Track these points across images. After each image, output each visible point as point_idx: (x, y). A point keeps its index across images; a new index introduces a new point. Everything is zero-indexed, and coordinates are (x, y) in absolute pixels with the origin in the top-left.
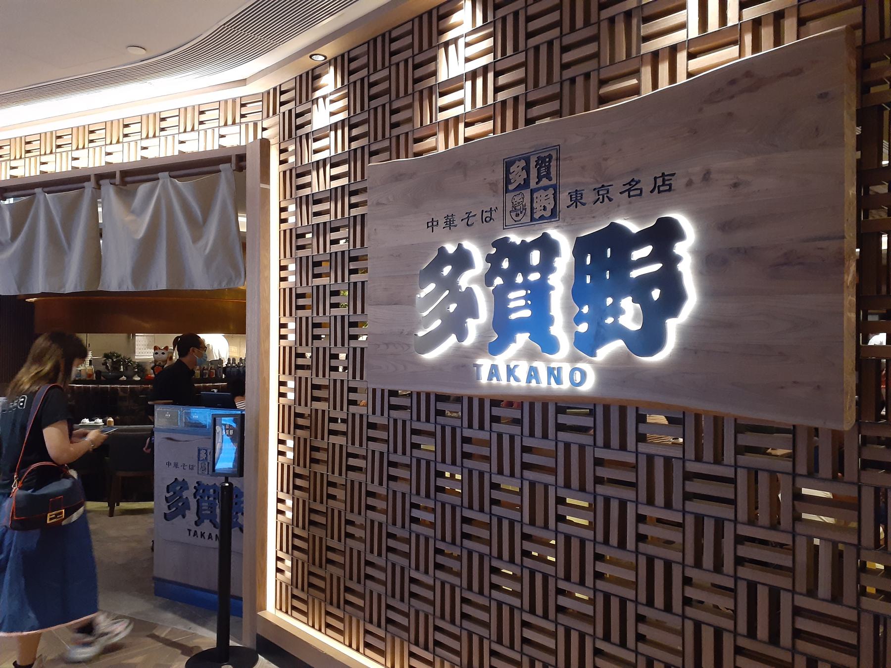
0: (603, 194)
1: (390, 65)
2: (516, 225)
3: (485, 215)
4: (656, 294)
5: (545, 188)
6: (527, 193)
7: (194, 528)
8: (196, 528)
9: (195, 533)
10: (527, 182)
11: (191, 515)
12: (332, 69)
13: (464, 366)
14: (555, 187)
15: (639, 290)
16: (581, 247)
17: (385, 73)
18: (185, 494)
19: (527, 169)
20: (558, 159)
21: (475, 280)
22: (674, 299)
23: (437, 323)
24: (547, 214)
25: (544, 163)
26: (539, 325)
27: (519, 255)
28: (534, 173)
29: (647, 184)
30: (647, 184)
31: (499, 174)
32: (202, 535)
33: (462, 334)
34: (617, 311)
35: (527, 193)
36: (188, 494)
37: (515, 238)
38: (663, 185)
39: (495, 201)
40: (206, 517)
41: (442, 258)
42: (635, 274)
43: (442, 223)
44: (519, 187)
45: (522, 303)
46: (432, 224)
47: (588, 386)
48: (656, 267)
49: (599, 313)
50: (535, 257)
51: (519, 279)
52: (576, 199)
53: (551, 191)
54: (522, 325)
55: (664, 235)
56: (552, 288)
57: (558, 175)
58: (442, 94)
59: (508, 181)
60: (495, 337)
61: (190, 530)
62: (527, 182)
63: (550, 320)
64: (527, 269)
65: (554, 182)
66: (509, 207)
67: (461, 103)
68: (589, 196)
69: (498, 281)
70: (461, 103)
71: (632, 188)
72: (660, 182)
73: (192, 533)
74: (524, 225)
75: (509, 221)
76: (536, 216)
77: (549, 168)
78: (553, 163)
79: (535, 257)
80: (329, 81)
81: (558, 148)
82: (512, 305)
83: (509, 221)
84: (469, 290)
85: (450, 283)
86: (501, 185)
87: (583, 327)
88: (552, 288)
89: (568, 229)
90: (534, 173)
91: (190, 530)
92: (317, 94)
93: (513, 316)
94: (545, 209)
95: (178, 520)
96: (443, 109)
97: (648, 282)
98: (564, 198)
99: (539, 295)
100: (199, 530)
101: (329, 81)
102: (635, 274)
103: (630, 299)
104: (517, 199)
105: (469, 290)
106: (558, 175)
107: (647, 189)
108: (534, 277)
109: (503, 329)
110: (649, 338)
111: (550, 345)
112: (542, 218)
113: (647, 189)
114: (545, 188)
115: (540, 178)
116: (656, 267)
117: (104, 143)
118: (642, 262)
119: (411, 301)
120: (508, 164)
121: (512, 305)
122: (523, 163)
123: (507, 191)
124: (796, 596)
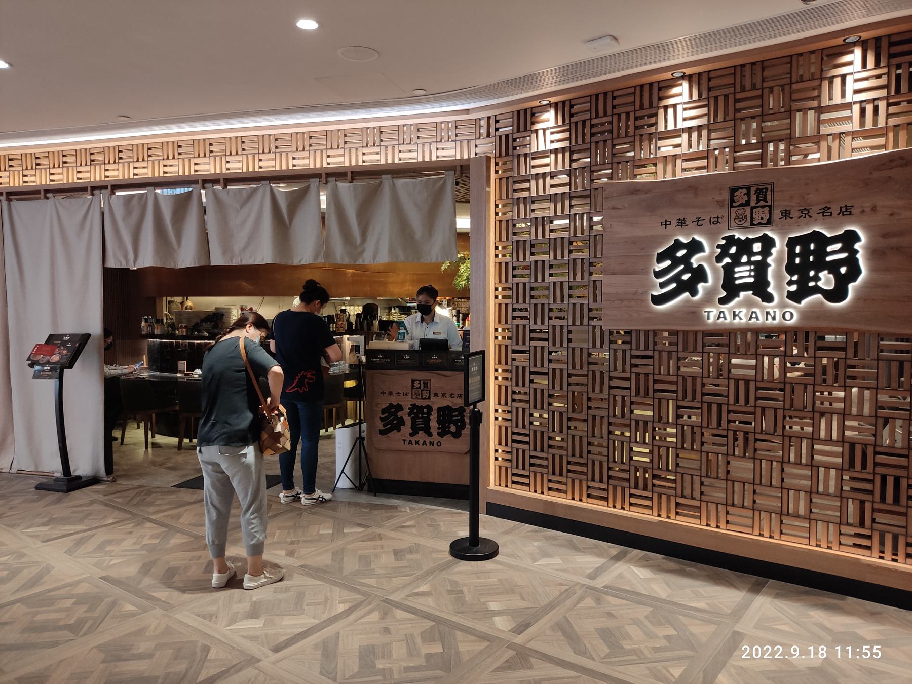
0: (805, 213)
1: (612, 115)
2: (739, 227)
3: (712, 220)
4: (843, 270)
5: (763, 207)
6: (748, 209)
7: (409, 438)
8: (411, 438)
9: (410, 442)
10: (748, 203)
11: (406, 429)
12: (552, 112)
13: (693, 312)
14: (770, 207)
15: (833, 267)
16: (792, 243)
17: (609, 119)
18: (400, 414)
19: (748, 194)
20: (772, 191)
21: (708, 259)
22: (854, 272)
23: (674, 285)
24: (764, 221)
25: (762, 193)
26: (760, 288)
27: (745, 247)
28: (753, 197)
29: (835, 210)
30: (835, 210)
31: (726, 195)
32: (417, 443)
33: (694, 293)
34: (816, 278)
35: (748, 209)
36: (404, 414)
37: (739, 235)
38: (846, 212)
39: (723, 212)
40: (421, 429)
41: (678, 245)
42: (829, 259)
43: (675, 223)
44: (741, 205)
45: (747, 274)
46: (666, 224)
47: (793, 322)
48: (843, 255)
49: (803, 283)
50: (757, 247)
51: (744, 259)
52: (786, 214)
53: (767, 209)
54: (745, 287)
55: (849, 239)
56: (769, 265)
57: (772, 200)
58: (534, 159)
59: (732, 201)
60: (724, 294)
61: (404, 441)
62: (748, 203)
63: (767, 284)
64: (751, 254)
65: (769, 203)
66: (733, 215)
67: (548, 165)
68: (795, 213)
69: (727, 260)
70: (548, 165)
71: (825, 212)
72: (843, 210)
73: (407, 443)
74: (746, 227)
75: (733, 224)
76: (755, 223)
77: (765, 195)
78: (769, 193)
79: (757, 247)
80: (549, 119)
81: (772, 184)
82: (736, 275)
83: (733, 224)
84: (700, 267)
85: (686, 260)
86: (727, 202)
87: (794, 288)
88: (769, 265)
89: (782, 234)
90: (753, 197)
91: (404, 441)
92: (538, 126)
93: (737, 282)
94: (762, 219)
95: (394, 434)
96: (534, 167)
97: (840, 263)
98: (777, 214)
99: (761, 269)
100: (413, 439)
101: (549, 119)
102: (829, 259)
103: (826, 272)
104: (740, 212)
105: (700, 267)
106: (772, 200)
107: (835, 212)
108: (758, 258)
109: (731, 289)
110: (837, 294)
111: (768, 298)
112: (760, 224)
113: (835, 212)
114: (763, 207)
115: (758, 201)
116: (843, 255)
117: (788, 81)
118: (835, 253)
119: (645, 271)
120: (733, 191)
121: (736, 275)
122: (745, 191)
123: (732, 206)
124: (783, 517)
